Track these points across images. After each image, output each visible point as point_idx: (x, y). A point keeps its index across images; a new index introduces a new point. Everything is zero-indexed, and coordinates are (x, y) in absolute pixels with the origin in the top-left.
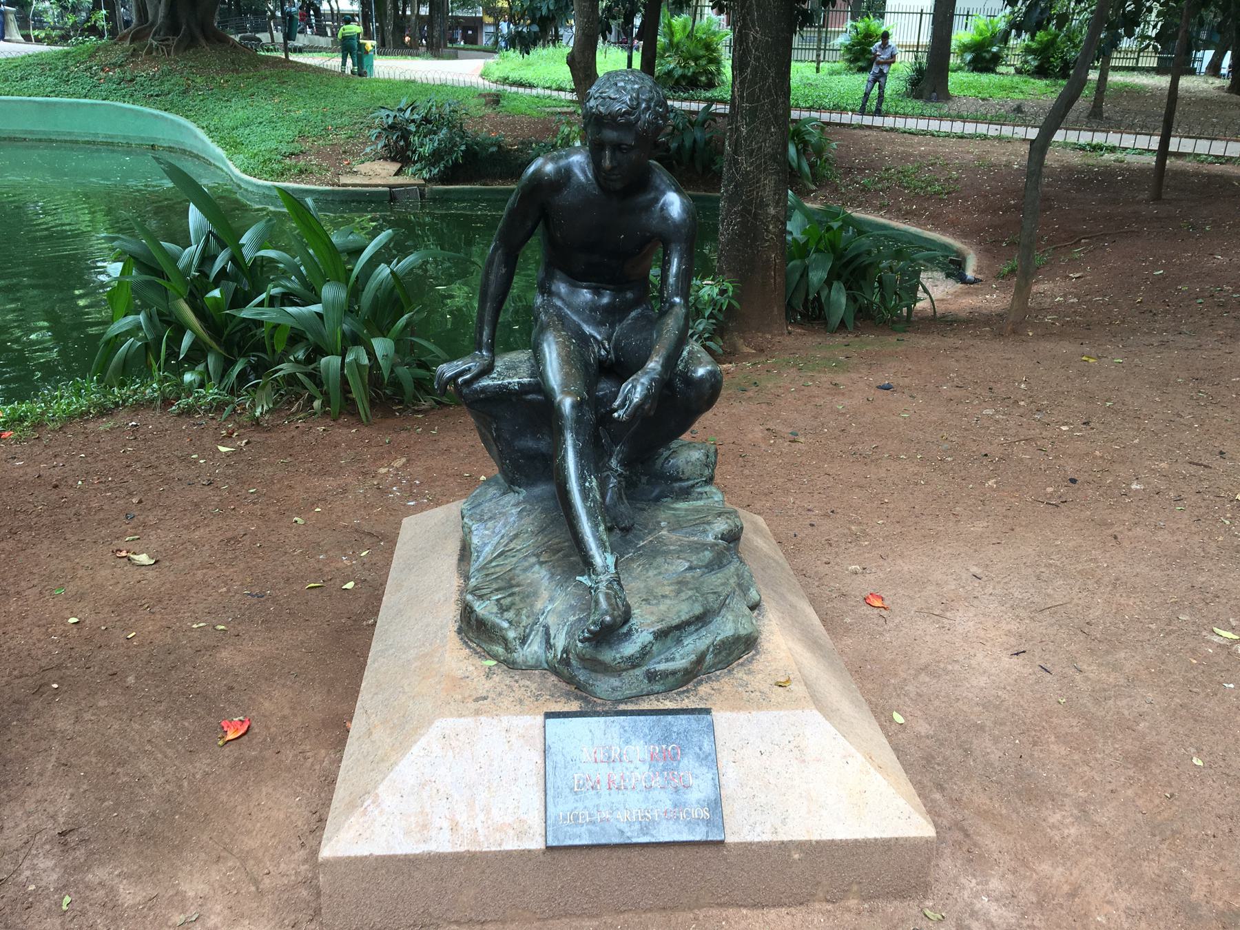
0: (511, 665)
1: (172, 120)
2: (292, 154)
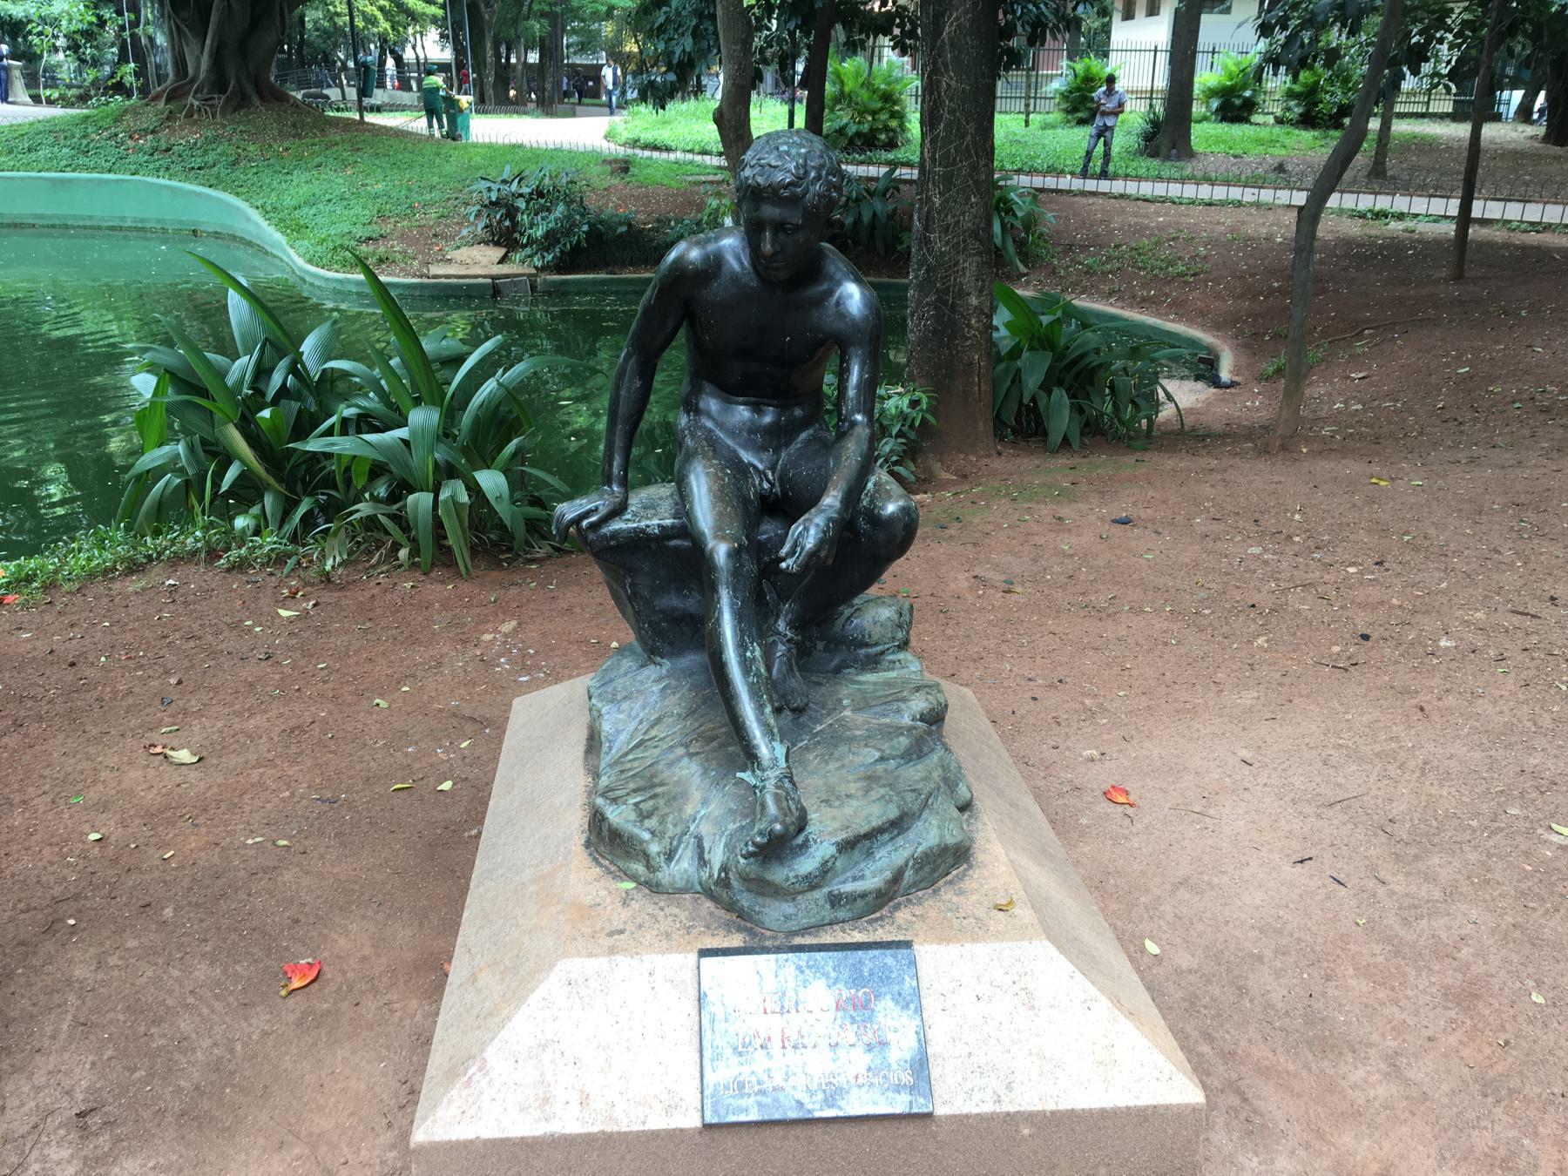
0: (654, 888)
1: (218, 199)
2: (370, 239)
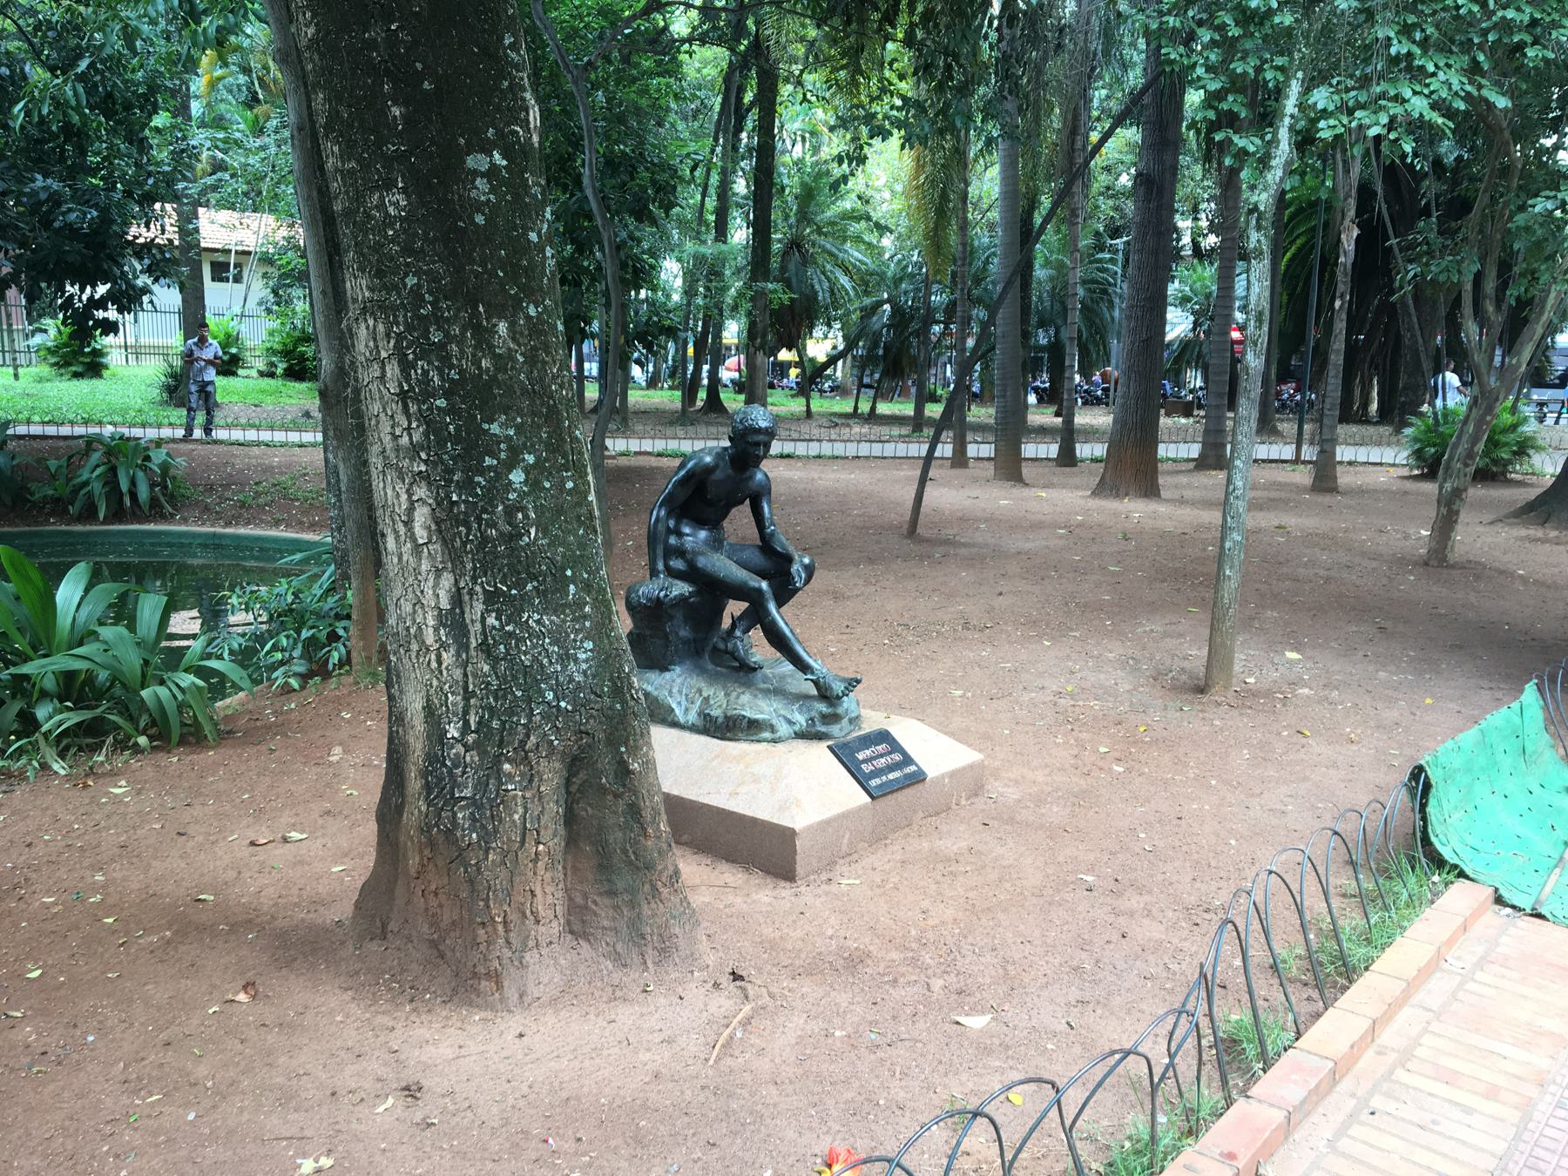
0: (774, 741)
